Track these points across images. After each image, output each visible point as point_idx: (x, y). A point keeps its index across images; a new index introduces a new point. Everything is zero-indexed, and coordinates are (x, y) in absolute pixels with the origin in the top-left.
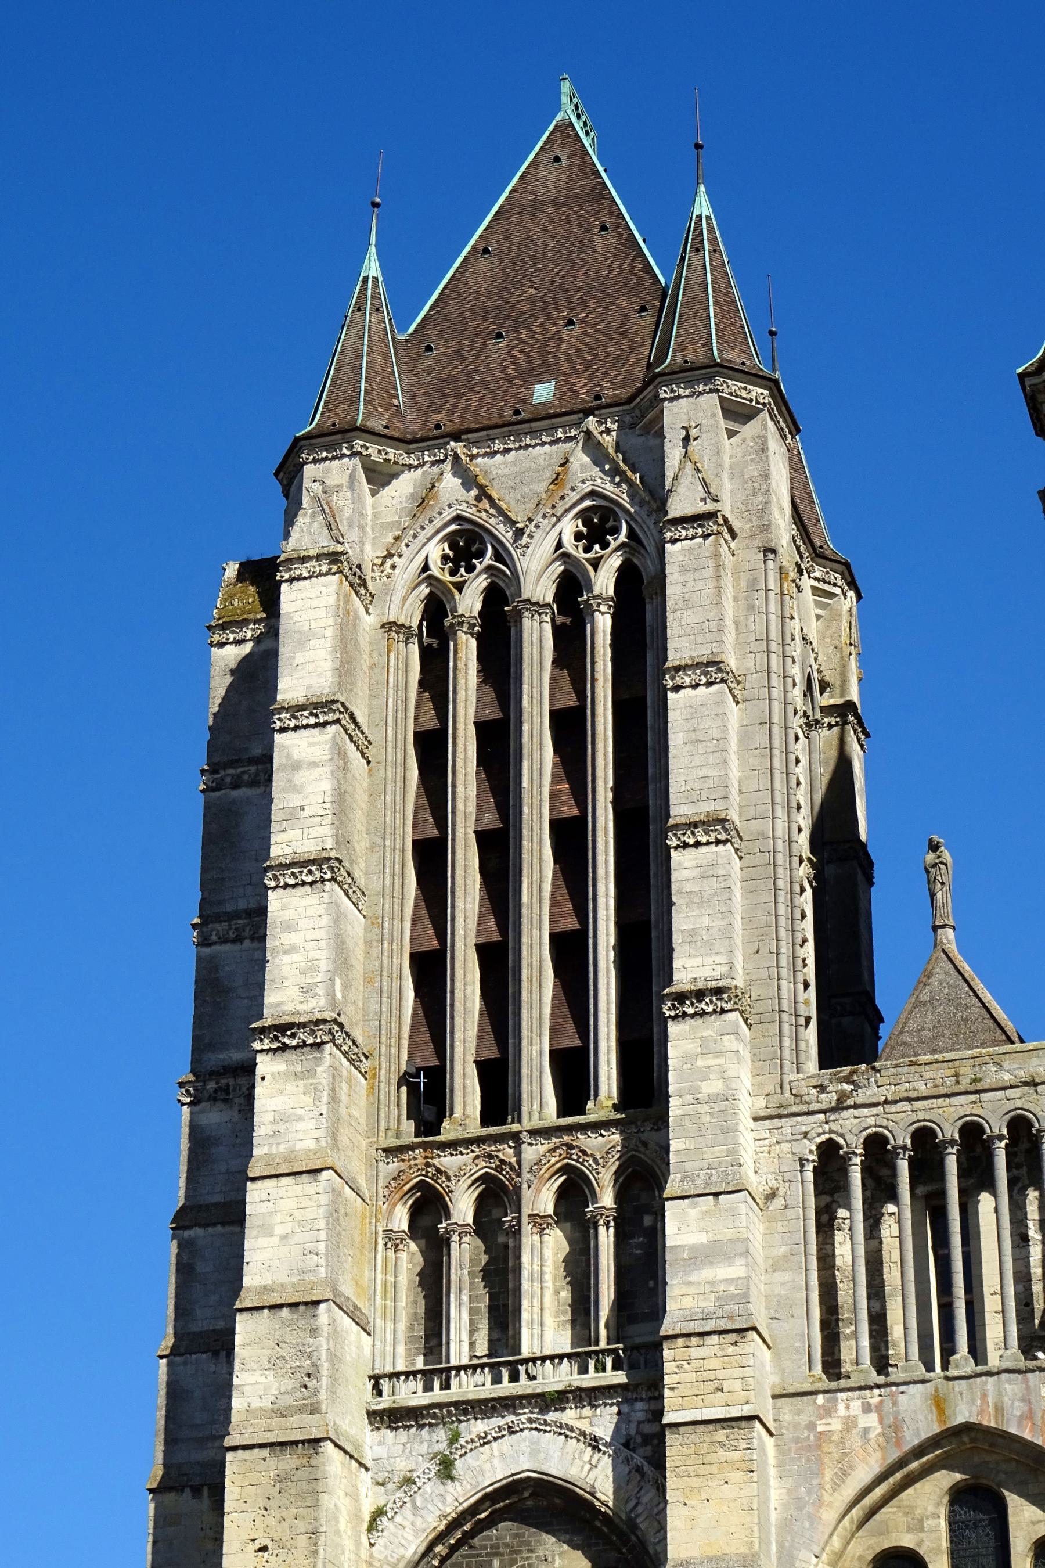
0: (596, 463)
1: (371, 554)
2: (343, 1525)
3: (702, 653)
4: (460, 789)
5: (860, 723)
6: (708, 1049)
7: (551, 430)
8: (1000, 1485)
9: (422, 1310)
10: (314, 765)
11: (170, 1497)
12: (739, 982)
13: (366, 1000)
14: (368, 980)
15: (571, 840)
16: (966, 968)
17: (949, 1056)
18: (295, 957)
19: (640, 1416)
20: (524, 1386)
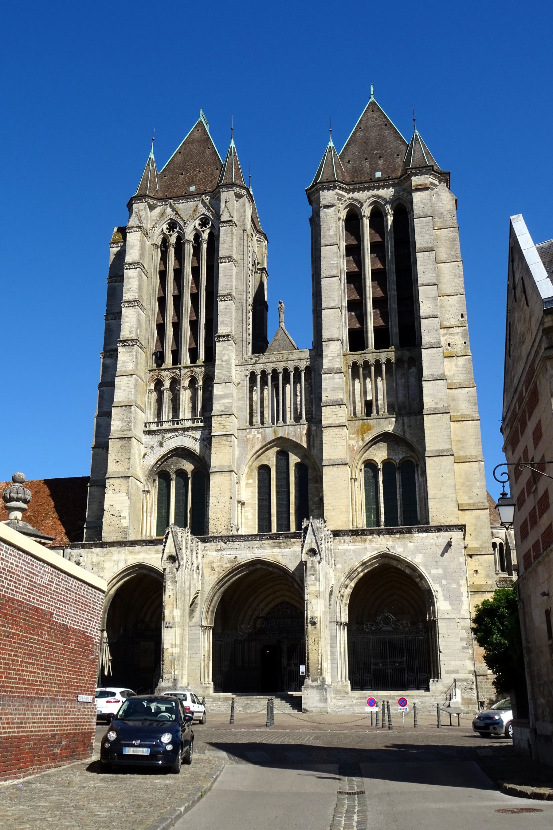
0: (205, 207)
1: (149, 226)
2: (136, 457)
3: (227, 254)
4: (169, 285)
5: (267, 273)
6: (225, 349)
7: (194, 198)
8: (288, 451)
9: (157, 408)
10: (134, 278)
11: (97, 449)
12: (233, 334)
13: (145, 335)
14: (146, 330)
15: (195, 298)
16: (286, 332)
17: (281, 352)
18: (128, 324)
19: (206, 433)
20: (180, 426)
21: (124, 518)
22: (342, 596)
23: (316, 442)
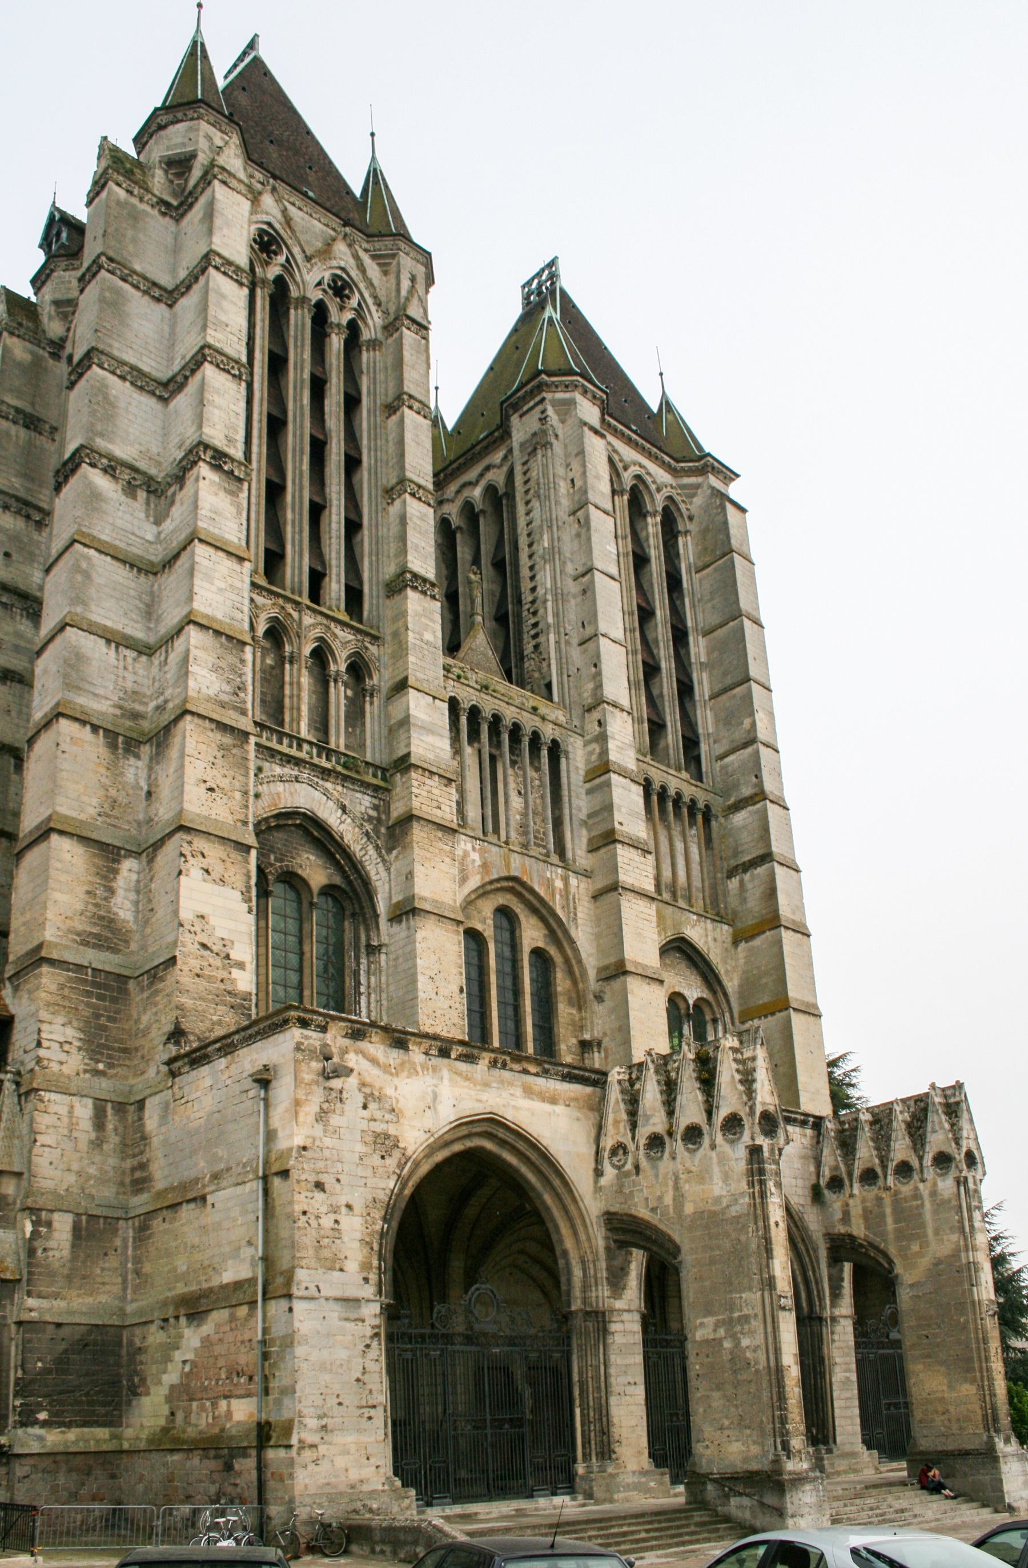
21: (241, 965)
23: (579, 915)
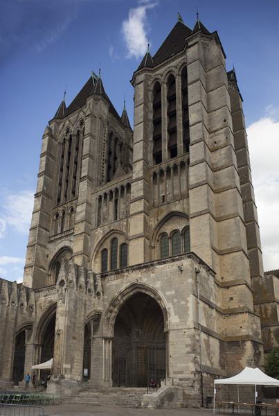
6: (84, 185)
22: (108, 319)
